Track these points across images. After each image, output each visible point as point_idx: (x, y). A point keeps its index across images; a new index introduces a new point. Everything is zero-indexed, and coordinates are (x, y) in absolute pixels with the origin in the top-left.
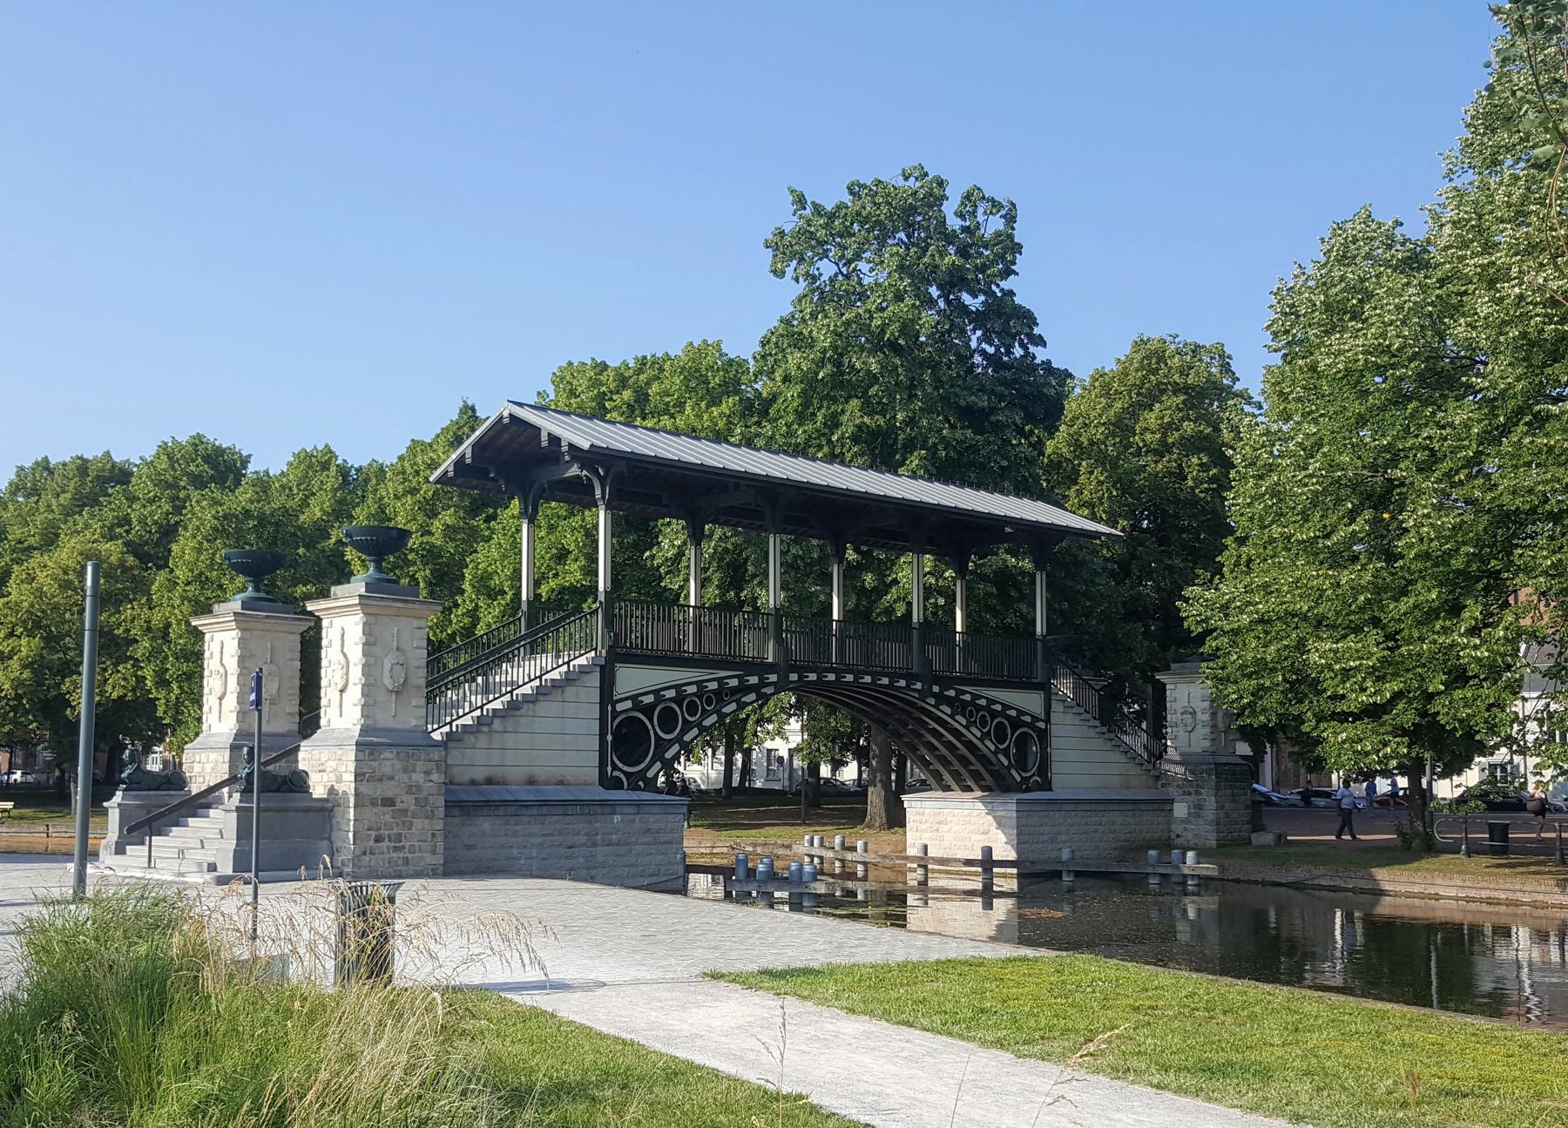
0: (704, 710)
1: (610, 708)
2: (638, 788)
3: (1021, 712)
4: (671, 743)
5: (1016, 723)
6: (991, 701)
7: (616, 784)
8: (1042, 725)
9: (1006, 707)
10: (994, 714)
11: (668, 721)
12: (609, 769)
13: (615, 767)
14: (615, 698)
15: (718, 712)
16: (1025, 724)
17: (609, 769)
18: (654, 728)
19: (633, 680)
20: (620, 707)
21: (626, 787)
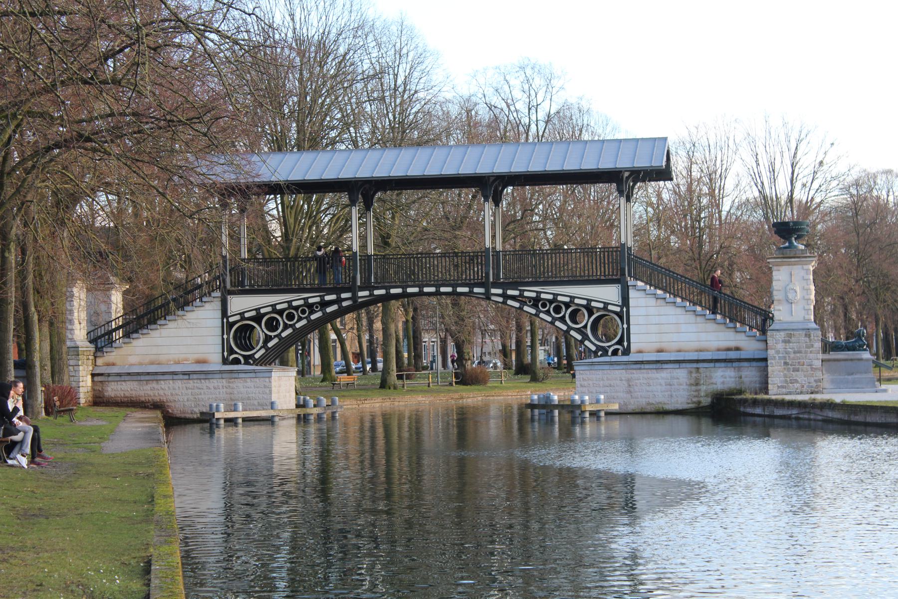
1: (225, 320)
2: (249, 364)
3: (589, 301)
7: (236, 362)
8: (618, 309)
9: (572, 298)
10: (567, 305)
11: (272, 325)
12: (226, 354)
13: (231, 351)
14: (229, 314)
17: (226, 354)
19: (240, 304)
20: (231, 320)
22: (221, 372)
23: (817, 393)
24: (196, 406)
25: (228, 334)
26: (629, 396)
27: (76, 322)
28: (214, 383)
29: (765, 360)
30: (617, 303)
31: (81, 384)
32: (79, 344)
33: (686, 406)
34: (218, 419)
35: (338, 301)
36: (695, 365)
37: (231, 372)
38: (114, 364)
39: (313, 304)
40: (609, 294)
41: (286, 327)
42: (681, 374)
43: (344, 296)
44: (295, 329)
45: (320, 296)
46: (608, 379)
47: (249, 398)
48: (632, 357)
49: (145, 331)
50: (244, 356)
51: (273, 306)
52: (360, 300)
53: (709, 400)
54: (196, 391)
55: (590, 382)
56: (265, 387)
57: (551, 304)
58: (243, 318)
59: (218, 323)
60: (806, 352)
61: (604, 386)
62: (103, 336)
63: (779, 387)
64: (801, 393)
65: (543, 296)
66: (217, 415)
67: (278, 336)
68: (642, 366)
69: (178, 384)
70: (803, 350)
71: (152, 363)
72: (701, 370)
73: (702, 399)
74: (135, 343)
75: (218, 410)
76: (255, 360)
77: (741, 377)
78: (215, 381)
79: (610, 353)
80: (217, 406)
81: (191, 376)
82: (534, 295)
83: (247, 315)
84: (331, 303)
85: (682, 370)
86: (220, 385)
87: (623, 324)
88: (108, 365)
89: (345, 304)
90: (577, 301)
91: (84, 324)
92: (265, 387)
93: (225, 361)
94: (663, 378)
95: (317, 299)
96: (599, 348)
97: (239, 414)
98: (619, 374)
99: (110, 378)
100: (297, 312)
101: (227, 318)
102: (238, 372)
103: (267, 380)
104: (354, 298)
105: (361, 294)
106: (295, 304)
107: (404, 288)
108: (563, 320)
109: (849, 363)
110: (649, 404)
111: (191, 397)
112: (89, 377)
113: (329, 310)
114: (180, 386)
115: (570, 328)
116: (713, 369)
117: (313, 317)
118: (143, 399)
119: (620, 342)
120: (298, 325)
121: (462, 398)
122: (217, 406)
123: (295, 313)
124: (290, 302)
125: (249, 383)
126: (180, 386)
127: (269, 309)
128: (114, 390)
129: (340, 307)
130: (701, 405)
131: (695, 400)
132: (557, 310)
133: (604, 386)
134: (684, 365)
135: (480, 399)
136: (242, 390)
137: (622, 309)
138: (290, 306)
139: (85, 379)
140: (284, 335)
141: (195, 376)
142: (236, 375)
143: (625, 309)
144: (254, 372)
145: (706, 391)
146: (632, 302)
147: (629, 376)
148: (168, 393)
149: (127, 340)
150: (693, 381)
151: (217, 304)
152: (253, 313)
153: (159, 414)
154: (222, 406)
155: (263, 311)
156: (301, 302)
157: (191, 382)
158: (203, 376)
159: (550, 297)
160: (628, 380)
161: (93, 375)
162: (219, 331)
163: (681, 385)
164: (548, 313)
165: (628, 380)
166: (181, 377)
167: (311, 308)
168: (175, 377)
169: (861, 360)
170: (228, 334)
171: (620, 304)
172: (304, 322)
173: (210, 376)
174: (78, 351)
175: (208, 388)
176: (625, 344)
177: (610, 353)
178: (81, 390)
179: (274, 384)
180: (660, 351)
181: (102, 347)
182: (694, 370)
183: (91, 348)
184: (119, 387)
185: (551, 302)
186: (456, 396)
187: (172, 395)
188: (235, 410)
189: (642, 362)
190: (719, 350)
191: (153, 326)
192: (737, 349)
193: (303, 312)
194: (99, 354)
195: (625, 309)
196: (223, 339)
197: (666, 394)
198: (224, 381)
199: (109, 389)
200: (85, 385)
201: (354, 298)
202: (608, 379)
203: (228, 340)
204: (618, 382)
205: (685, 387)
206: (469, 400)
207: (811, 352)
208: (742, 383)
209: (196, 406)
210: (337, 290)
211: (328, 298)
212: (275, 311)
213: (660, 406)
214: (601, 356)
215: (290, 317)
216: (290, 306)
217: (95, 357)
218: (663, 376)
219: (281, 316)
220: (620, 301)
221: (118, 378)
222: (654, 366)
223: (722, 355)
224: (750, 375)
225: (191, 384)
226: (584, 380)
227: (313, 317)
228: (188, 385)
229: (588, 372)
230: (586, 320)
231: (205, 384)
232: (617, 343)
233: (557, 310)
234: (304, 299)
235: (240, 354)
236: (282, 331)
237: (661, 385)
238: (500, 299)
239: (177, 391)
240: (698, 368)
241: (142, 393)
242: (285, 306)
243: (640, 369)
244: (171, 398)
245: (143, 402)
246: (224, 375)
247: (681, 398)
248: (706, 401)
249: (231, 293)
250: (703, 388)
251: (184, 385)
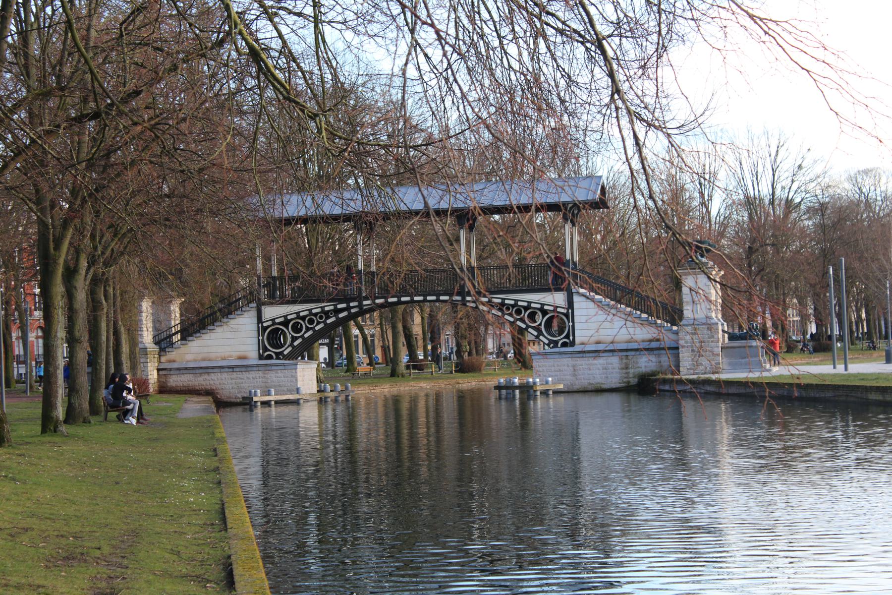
1: (260, 325)
2: (280, 359)
3: (542, 305)
4: (297, 338)
6: (516, 301)
7: (270, 357)
8: (565, 311)
9: (530, 303)
10: (526, 308)
11: (297, 329)
13: (265, 349)
15: (324, 322)
17: (261, 351)
19: (272, 312)
20: (265, 325)
21: (274, 356)
22: (258, 366)
23: (717, 373)
24: (238, 393)
25: (263, 336)
26: (574, 378)
27: (145, 329)
28: (252, 374)
29: (677, 348)
31: (150, 377)
32: (147, 345)
33: (618, 385)
34: (256, 402)
35: (348, 309)
36: (625, 353)
37: (266, 365)
38: (174, 361)
39: (328, 311)
40: (557, 299)
41: (308, 329)
42: (614, 361)
43: (352, 304)
44: (315, 331)
46: (558, 366)
47: (280, 386)
48: (577, 348)
49: (198, 335)
50: (275, 353)
51: (298, 313)
52: (365, 308)
53: (636, 380)
54: (240, 381)
55: (544, 368)
56: (292, 376)
58: (274, 323)
59: (255, 327)
60: (708, 342)
61: (555, 371)
62: (165, 339)
63: (688, 369)
64: (705, 373)
65: (507, 302)
66: (255, 399)
67: (302, 336)
68: (584, 355)
69: (225, 375)
70: (706, 340)
71: (204, 360)
72: (630, 357)
73: (631, 380)
74: (191, 344)
75: (256, 395)
76: (284, 356)
77: (660, 362)
78: (253, 373)
79: (559, 345)
80: (255, 392)
81: (235, 369)
82: (499, 301)
83: (277, 321)
84: (342, 310)
85: (615, 358)
86: (258, 375)
87: (569, 322)
88: (170, 361)
89: (353, 311)
90: (533, 305)
91: (151, 329)
92: (292, 376)
93: (261, 357)
94: (600, 364)
95: (332, 308)
96: (551, 342)
97: (272, 398)
98: (566, 361)
99: (172, 372)
101: (262, 323)
102: (271, 365)
103: (294, 371)
104: (360, 306)
105: (365, 303)
106: (314, 311)
107: (399, 298)
108: (522, 320)
109: (742, 349)
110: (590, 384)
111: (235, 386)
112: (155, 372)
113: (341, 315)
114: (227, 377)
115: (528, 326)
116: (638, 357)
117: (329, 321)
118: (197, 388)
119: (567, 337)
120: (317, 328)
121: (458, 383)
122: (255, 392)
124: (310, 310)
125: (280, 374)
126: (227, 377)
127: (294, 316)
128: (175, 381)
129: (350, 313)
130: (631, 384)
131: (625, 380)
132: (518, 312)
133: (555, 371)
134: (616, 354)
135: (473, 384)
136: (274, 379)
137: (568, 311)
138: (311, 313)
139: (152, 373)
140: (306, 335)
141: (238, 369)
142: (269, 368)
143: (570, 311)
144: (284, 365)
145: (634, 373)
146: (576, 305)
147: (574, 363)
148: (217, 382)
149: (184, 342)
150: (623, 366)
151: (254, 313)
152: (282, 319)
153: (210, 398)
154: (259, 391)
155: (289, 317)
156: (319, 310)
157: (235, 374)
158: (243, 369)
159: (512, 302)
160: (574, 366)
161: (158, 370)
162: (255, 334)
163: (614, 369)
164: (511, 315)
165: (574, 366)
166: (227, 370)
167: (327, 314)
168: (222, 370)
169: (751, 347)
170: (263, 336)
172: (321, 326)
173: (249, 369)
174: (146, 352)
175: (248, 378)
176: (571, 338)
177: (559, 345)
178: (150, 381)
179: (299, 374)
180: (598, 343)
181: (165, 348)
182: (623, 357)
183: (156, 349)
184: (179, 379)
185: (513, 306)
186: (453, 382)
187: (220, 384)
188: (269, 395)
189: (584, 352)
190: (643, 341)
191: (204, 331)
192: (658, 340)
193: (321, 317)
194: (162, 353)
195: (570, 311)
196: (259, 340)
197: (603, 376)
198: (260, 372)
199: (171, 380)
200: (153, 376)
201: (360, 306)
202: (558, 366)
203: (263, 340)
204: (566, 368)
205: (617, 370)
206: (464, 385)
207: (712, 342)
208: (661, 366)
209: (238, 393)
210: (347, 300)
211: (340, 306)
212: (299, 317)
213: (599, 385)
214: (553, 347)
215: (311, 322)
216: (311, 313)
217: (160, 356)
218: (601, 362)
219: (304, 321)
221: (178, 372)
222: (593, 355)
223: (646, 345)
224: (666, 360)
225: (235, 375)
226: (539, 366)
227: (329, 321)
228: (232, 377)
229: (542, 360)
231: (245, 375)
232: (565, 338)
233: (518, 312)
234: (321, 307)
235: (272, 351)
236: (305, 332)
237: (599, 369)
238: (473, 305)
239: (224, 382)
240: (627, 356)
241: (197, 383)
242: (306, 313)
243: (583, 357)
244: (220, 387)
245: (197, 390)
246: (261, 368)
247: (614, 379)
248: (634, 381)
249: (264, 304)
250: (632, 371)
251: (229, 377)
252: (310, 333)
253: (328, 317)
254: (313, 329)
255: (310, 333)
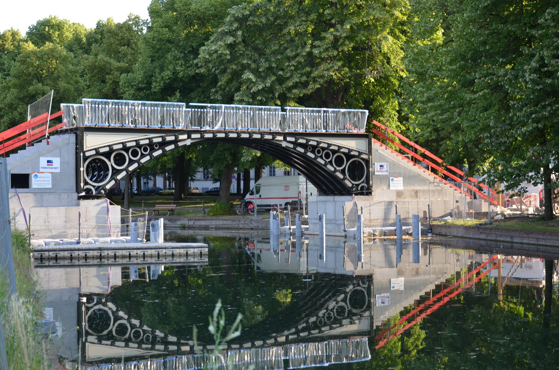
0: (142, 154)
1: (82, 154)
3: (350, 150)
4: (119, 172)
5: (349, 156)
6: (330, 145)
9: (340, 147)
10: (334, 152)
11: (120, 160)
12: (82, 184)
13: (86, 183)
15: (150, 155)
16: (354, 156)
18: (111, 163)
20: (87, 154)
30: (365, 152)
41: (131, 162)
45: (162, 137)
57: (323, 151)
58: (98, 153)
65: (322, 145)
67: (126, 169)
82: (315, 143)
83: (102, 150)
95: (160, 140)
100: (141, 150)
106: (142, 142)
108: (331, 163)
117: (155, 154)
123: (139, 150)
138: (138, 145)
152: (107, 149)
156: (147, 142)
159: (326, 146)
164: (321, 157)
171: (367, 153)
185: (324, 149)
193: (145, 150)
215: (135, 154)
219: (127, 153)
220: (367, 151)
227: (155, 154)
230: (346, 165)
234: (149, 139)
252: (135, 165)
253: (153, 150)
254: (138, 161)
255: (135, 165)
